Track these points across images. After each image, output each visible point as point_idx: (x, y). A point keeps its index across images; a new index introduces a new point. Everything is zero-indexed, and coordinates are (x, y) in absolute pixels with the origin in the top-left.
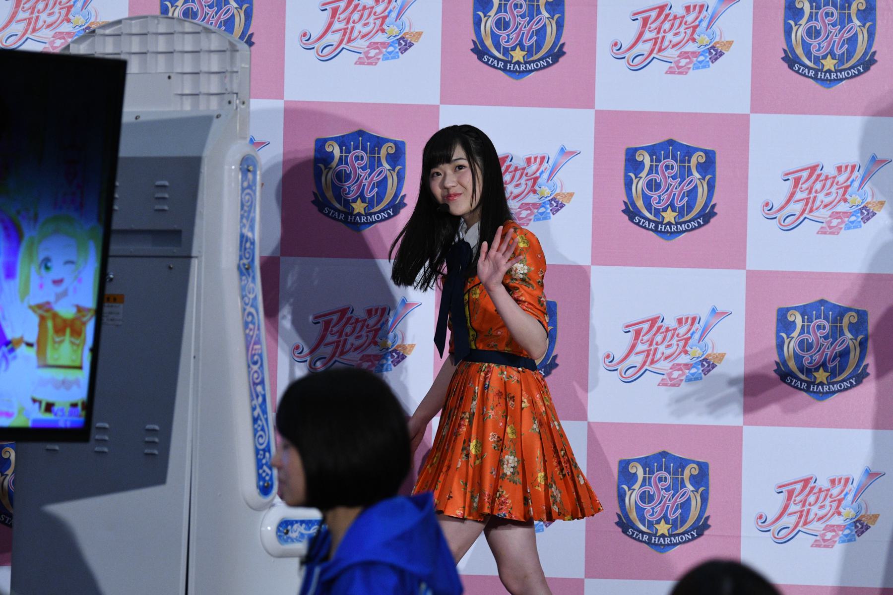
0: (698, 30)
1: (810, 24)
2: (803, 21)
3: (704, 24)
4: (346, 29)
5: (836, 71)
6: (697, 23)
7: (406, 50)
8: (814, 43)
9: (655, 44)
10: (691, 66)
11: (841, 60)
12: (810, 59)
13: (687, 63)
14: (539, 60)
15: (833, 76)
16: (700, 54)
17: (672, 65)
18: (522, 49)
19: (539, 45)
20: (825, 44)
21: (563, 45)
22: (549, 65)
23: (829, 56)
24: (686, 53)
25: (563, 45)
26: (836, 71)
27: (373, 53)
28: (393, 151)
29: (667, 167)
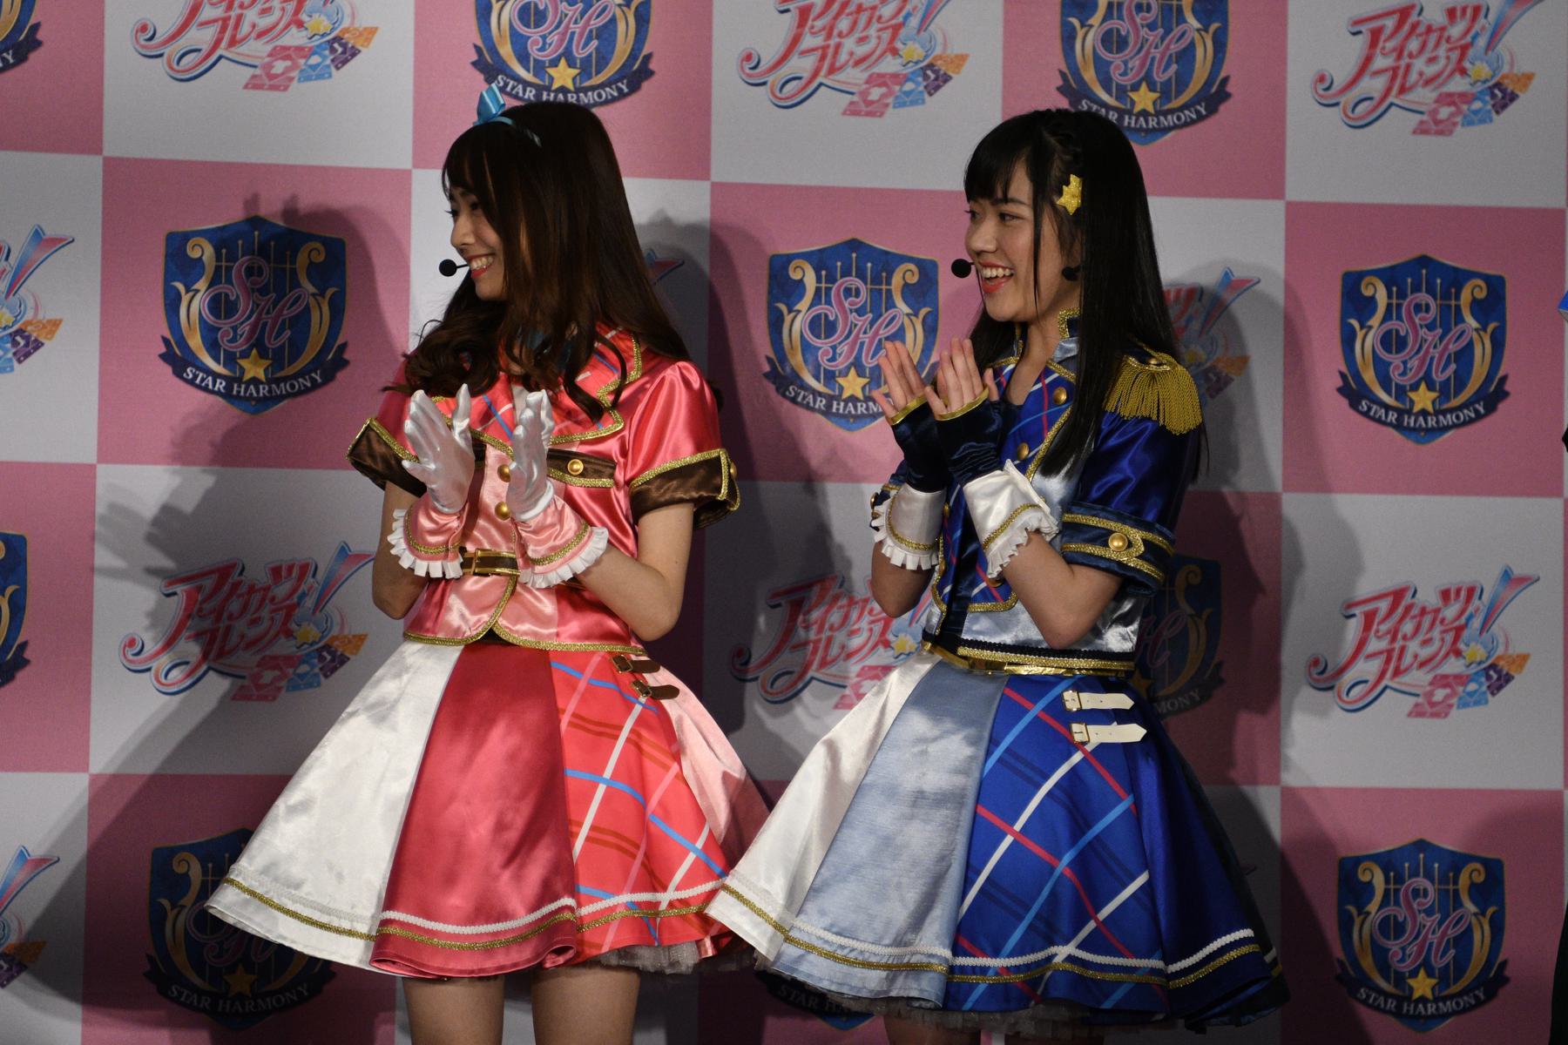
0: (903, 33)
1: (1108, 25)
2: (1096, 20)
3: (914, 22)
4: (225, 20)
5: (1158, 114)
6: (900, 19)
7: (345, 62)
8: (1116, 60)
9: (823, 58)
10: (890, 100)
11: (1166, 93)
12: (1109, 92)
13: (884, 96)
14: (602, 86)
15: (1152, 123)
16: (906, 79)
17: (855, 98)
18: (571, 64)
19: (603, 59)
20: (1135, 63)
21: (648, 57)
22: (622, 95)
23: (1144, 86)
24: (880, 75)
25: (648, 57)
26: (1158, 114)
27: (280, 66)
28: (321, 258)
29: (848, 292)
